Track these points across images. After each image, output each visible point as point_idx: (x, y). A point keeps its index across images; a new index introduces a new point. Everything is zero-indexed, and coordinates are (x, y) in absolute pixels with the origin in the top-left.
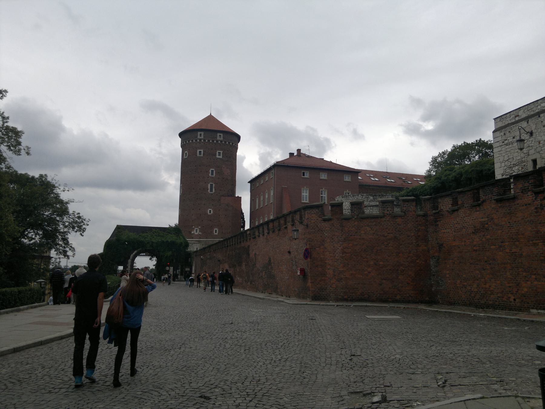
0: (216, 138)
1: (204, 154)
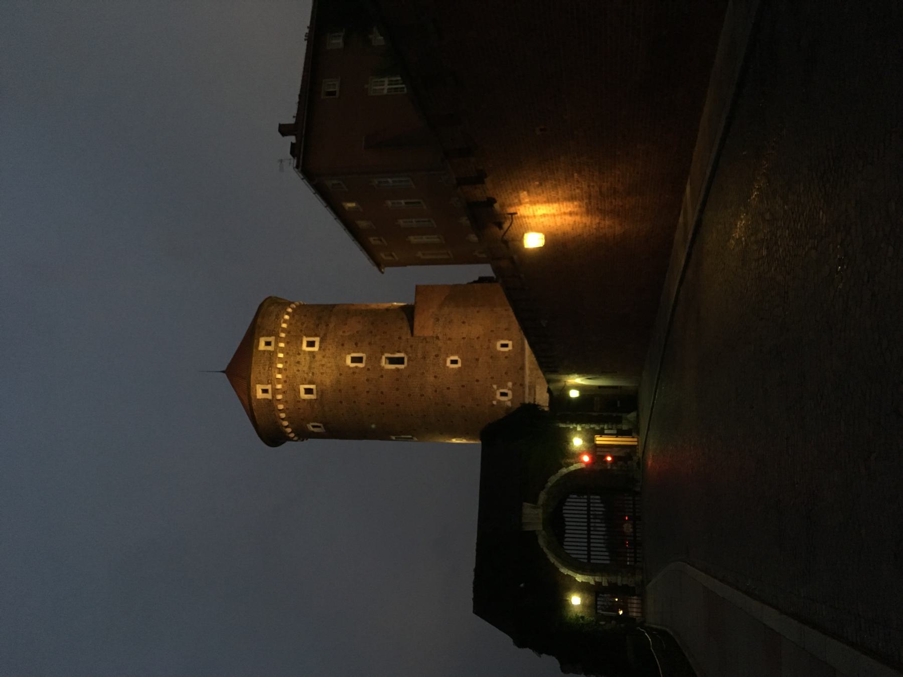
0: (269, 352)
1: (310, 383)
